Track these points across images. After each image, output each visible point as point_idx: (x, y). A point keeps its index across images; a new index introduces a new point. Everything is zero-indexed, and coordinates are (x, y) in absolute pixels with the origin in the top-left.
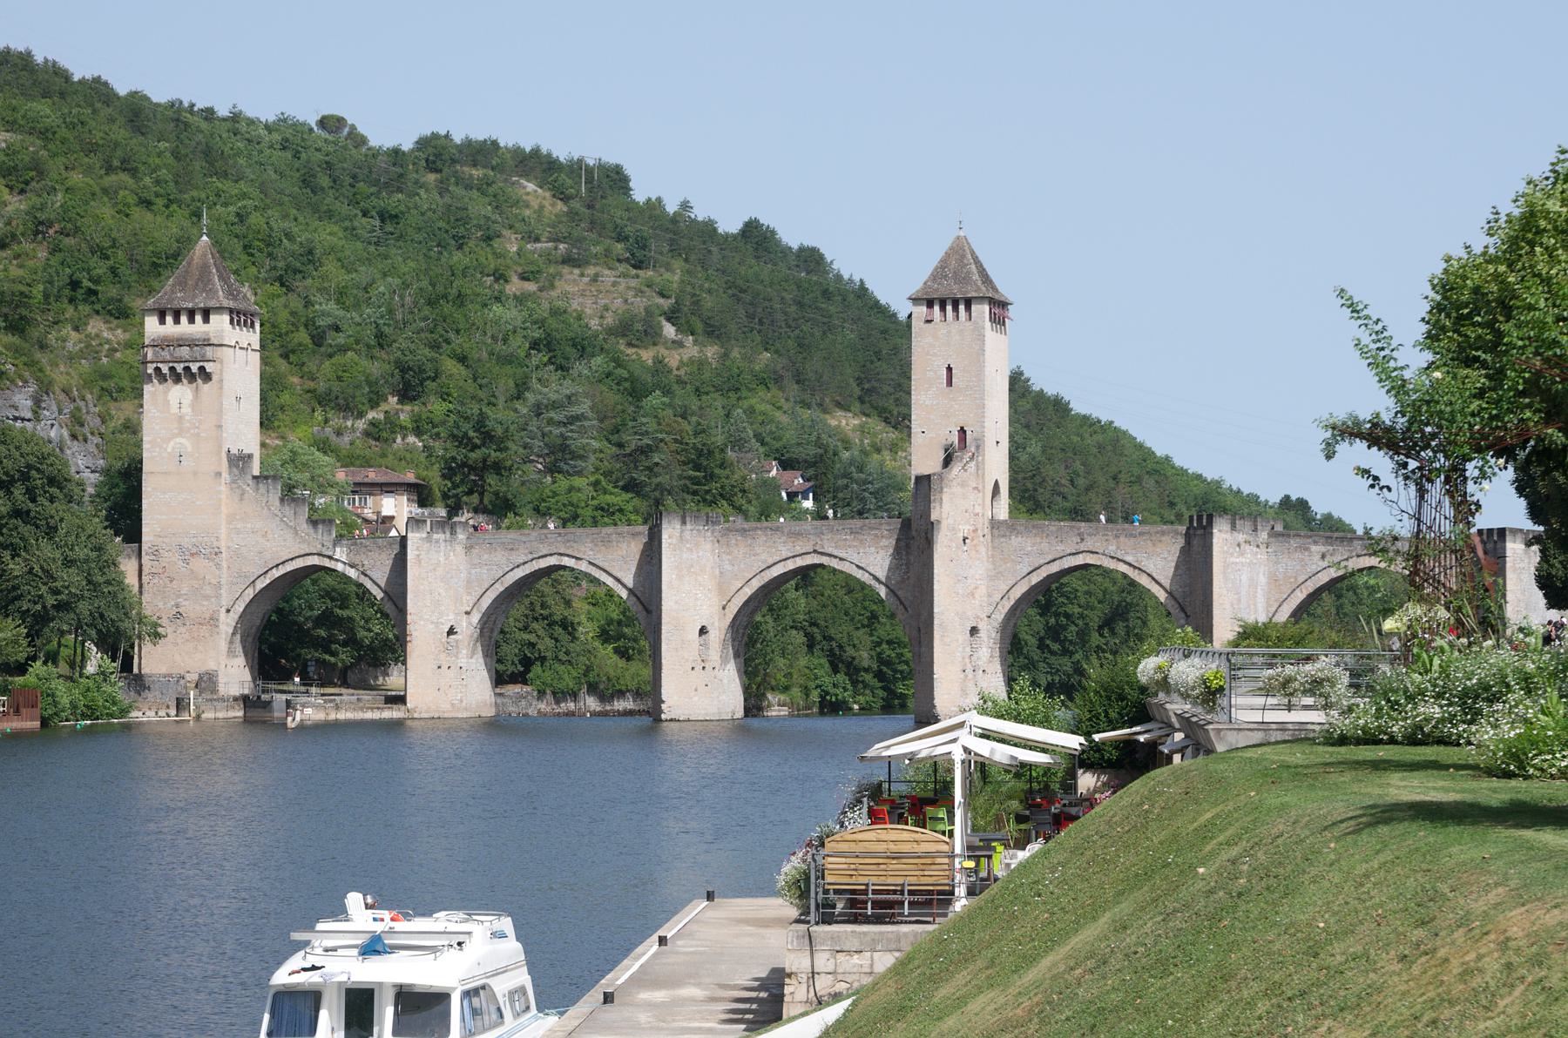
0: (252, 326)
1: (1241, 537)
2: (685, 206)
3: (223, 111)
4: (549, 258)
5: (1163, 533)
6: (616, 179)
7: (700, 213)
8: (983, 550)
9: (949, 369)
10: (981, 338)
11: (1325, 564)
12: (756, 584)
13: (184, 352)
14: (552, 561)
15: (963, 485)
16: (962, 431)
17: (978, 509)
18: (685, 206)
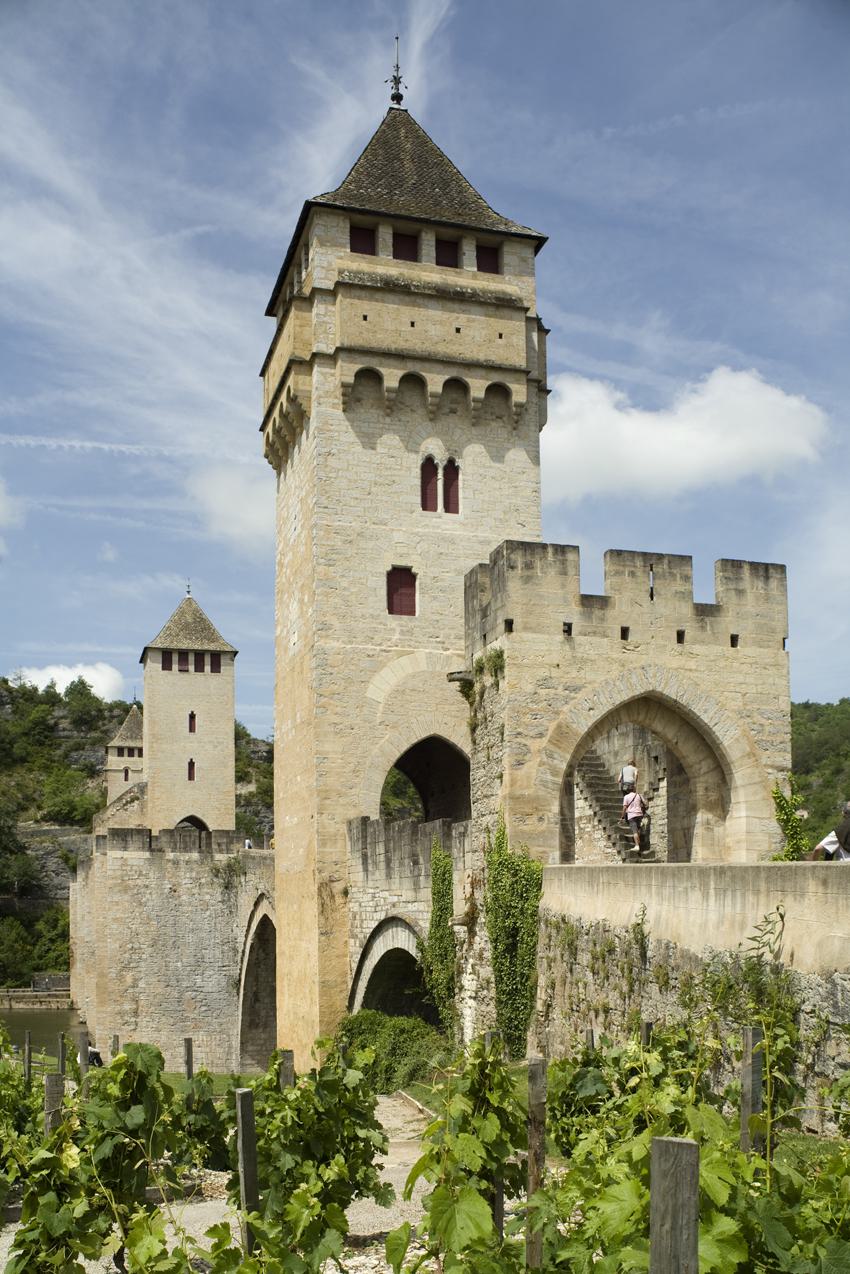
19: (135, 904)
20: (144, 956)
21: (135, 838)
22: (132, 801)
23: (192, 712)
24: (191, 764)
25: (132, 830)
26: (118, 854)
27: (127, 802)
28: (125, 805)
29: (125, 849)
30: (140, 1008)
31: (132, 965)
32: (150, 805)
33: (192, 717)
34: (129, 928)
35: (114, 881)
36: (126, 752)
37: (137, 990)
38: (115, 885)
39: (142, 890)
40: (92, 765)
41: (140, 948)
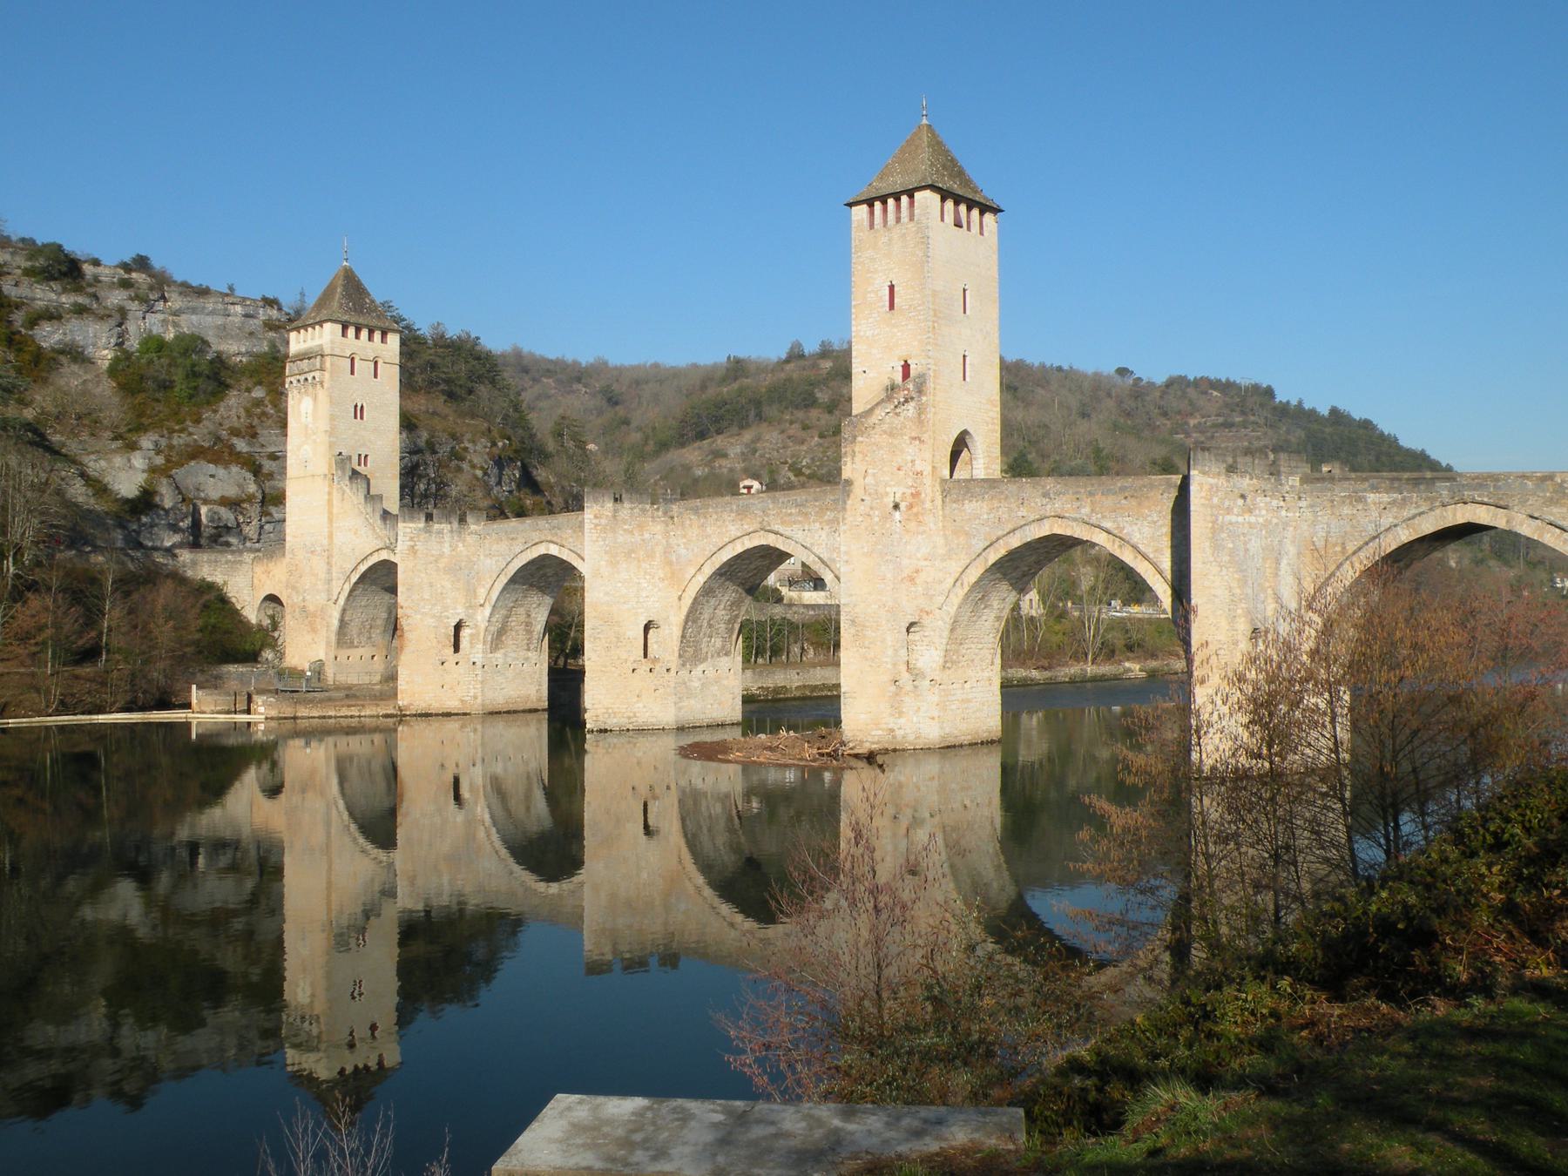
0: (383, 340)
1: (1245, 483)
2: (1300, 403)
3: (1066, 367)
4: (1214, 426)
5: (1152, 486)
6: (1269, 392)
7: (1307, 406)
9: (892, 288)
10: (925, 241)
11: (1387, 520)
12: (708, 570)
13: (305, 364)
14: (541, 550)
15: (891, 435)
16: (906, 367)
18: (1300, 403)
22: (906, 401)
36: (351, 331)
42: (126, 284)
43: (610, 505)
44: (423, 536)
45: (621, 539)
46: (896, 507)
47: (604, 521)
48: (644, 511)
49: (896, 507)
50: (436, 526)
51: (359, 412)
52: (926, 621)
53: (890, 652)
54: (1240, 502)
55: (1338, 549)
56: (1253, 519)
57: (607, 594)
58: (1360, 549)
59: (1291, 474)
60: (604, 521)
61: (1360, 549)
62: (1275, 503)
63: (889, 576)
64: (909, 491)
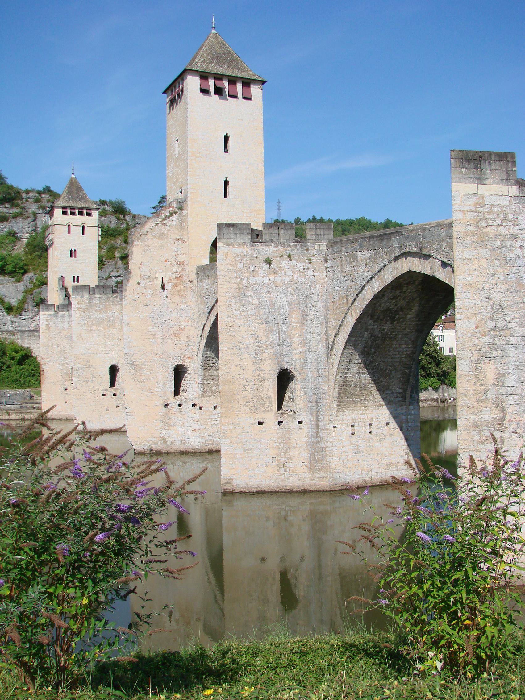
1: (269, 250)
8: (191, 296)
11: (367, 275)
15: (161, 237)
17: (181, 258)
19: (496, 262)
20: (513, 340)
21: (496, 165)
22: (171, 214)
23: (227, 134)
24: (226, 183)
25: (490, 154)
26: (471, 187)
27: (166, 217)
28: (163, 219)
29: (480, 180)
30: (508, 418)
31: (495, 354)
32: (190, 219)
33: (227, 138)
34: (489, 298)
35: (465, 228)
37: (503, 390)
38: (467, 234)
39: (509, 243)
40: (15, 233)
41: (506, 328)
42: (37, 201)
43: (86, 296)
44: (54, 319)
45: (94, 316)
46: (163, 287)
47: (83, 306)
48: (108, 298)
49: (163, 287)
50: (61, 313)
51: (72, 253)
52: (187, 364)
53: (161, 385)
54: (266, 266)
55: (345, 301)
56: (278, 279)
57: (86, 349)
58: (355, 300)
59: (317, 240)
60: (83, 306)
61: (355, 300)
62: (300, 265)
63: (159, 333)
64: (174, 276)
